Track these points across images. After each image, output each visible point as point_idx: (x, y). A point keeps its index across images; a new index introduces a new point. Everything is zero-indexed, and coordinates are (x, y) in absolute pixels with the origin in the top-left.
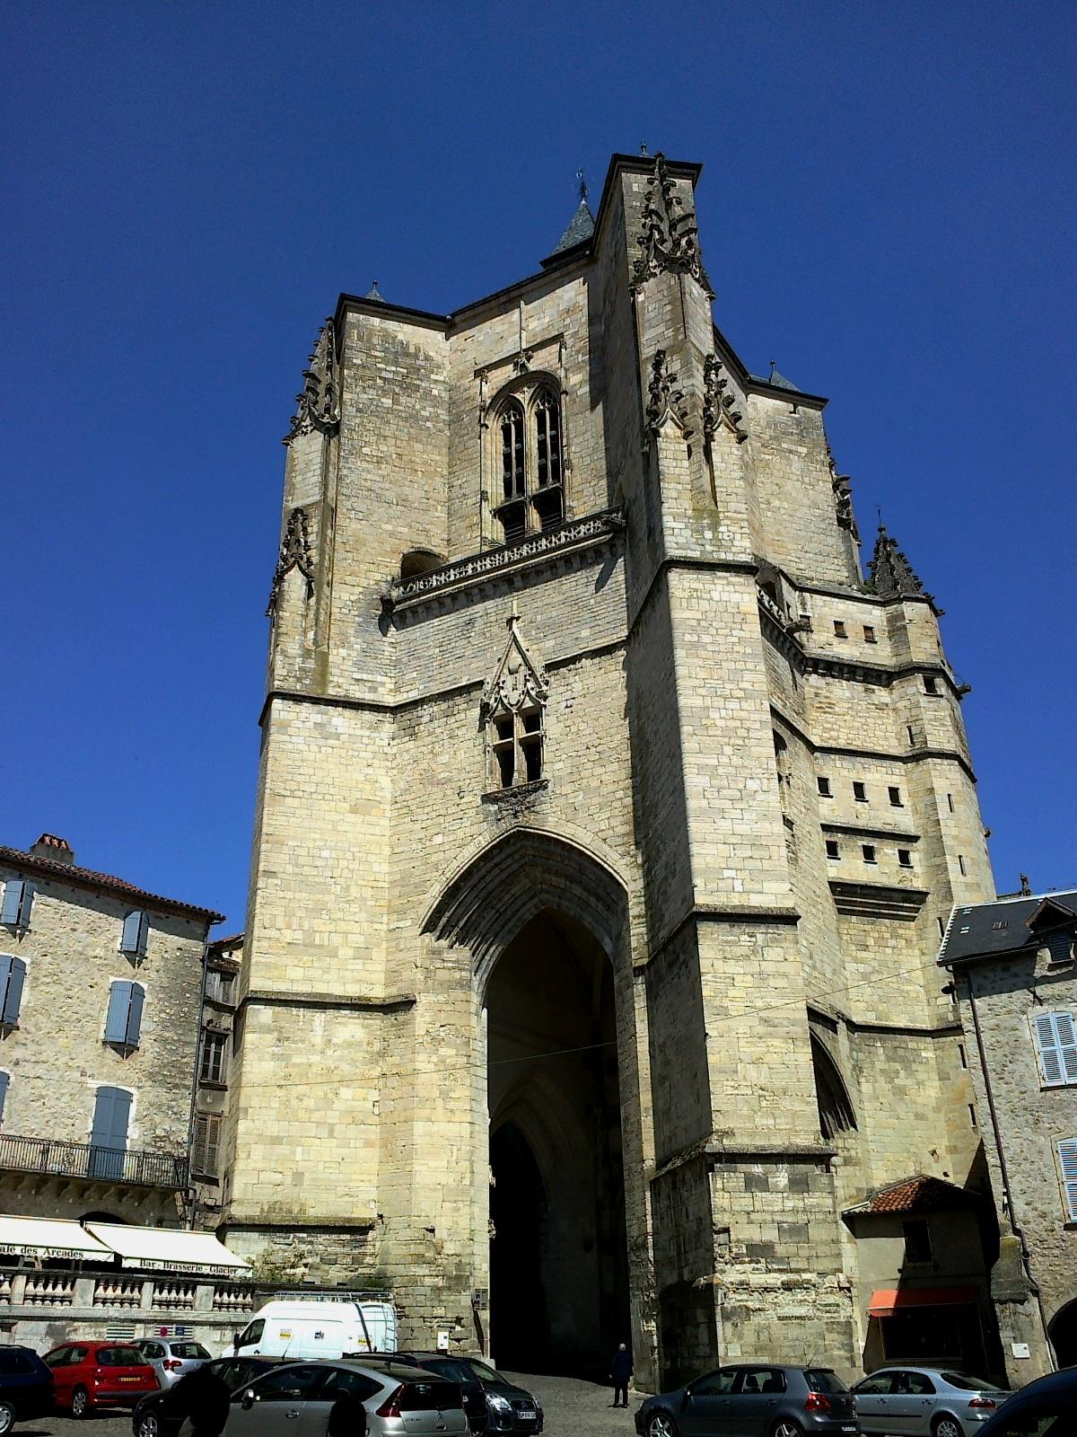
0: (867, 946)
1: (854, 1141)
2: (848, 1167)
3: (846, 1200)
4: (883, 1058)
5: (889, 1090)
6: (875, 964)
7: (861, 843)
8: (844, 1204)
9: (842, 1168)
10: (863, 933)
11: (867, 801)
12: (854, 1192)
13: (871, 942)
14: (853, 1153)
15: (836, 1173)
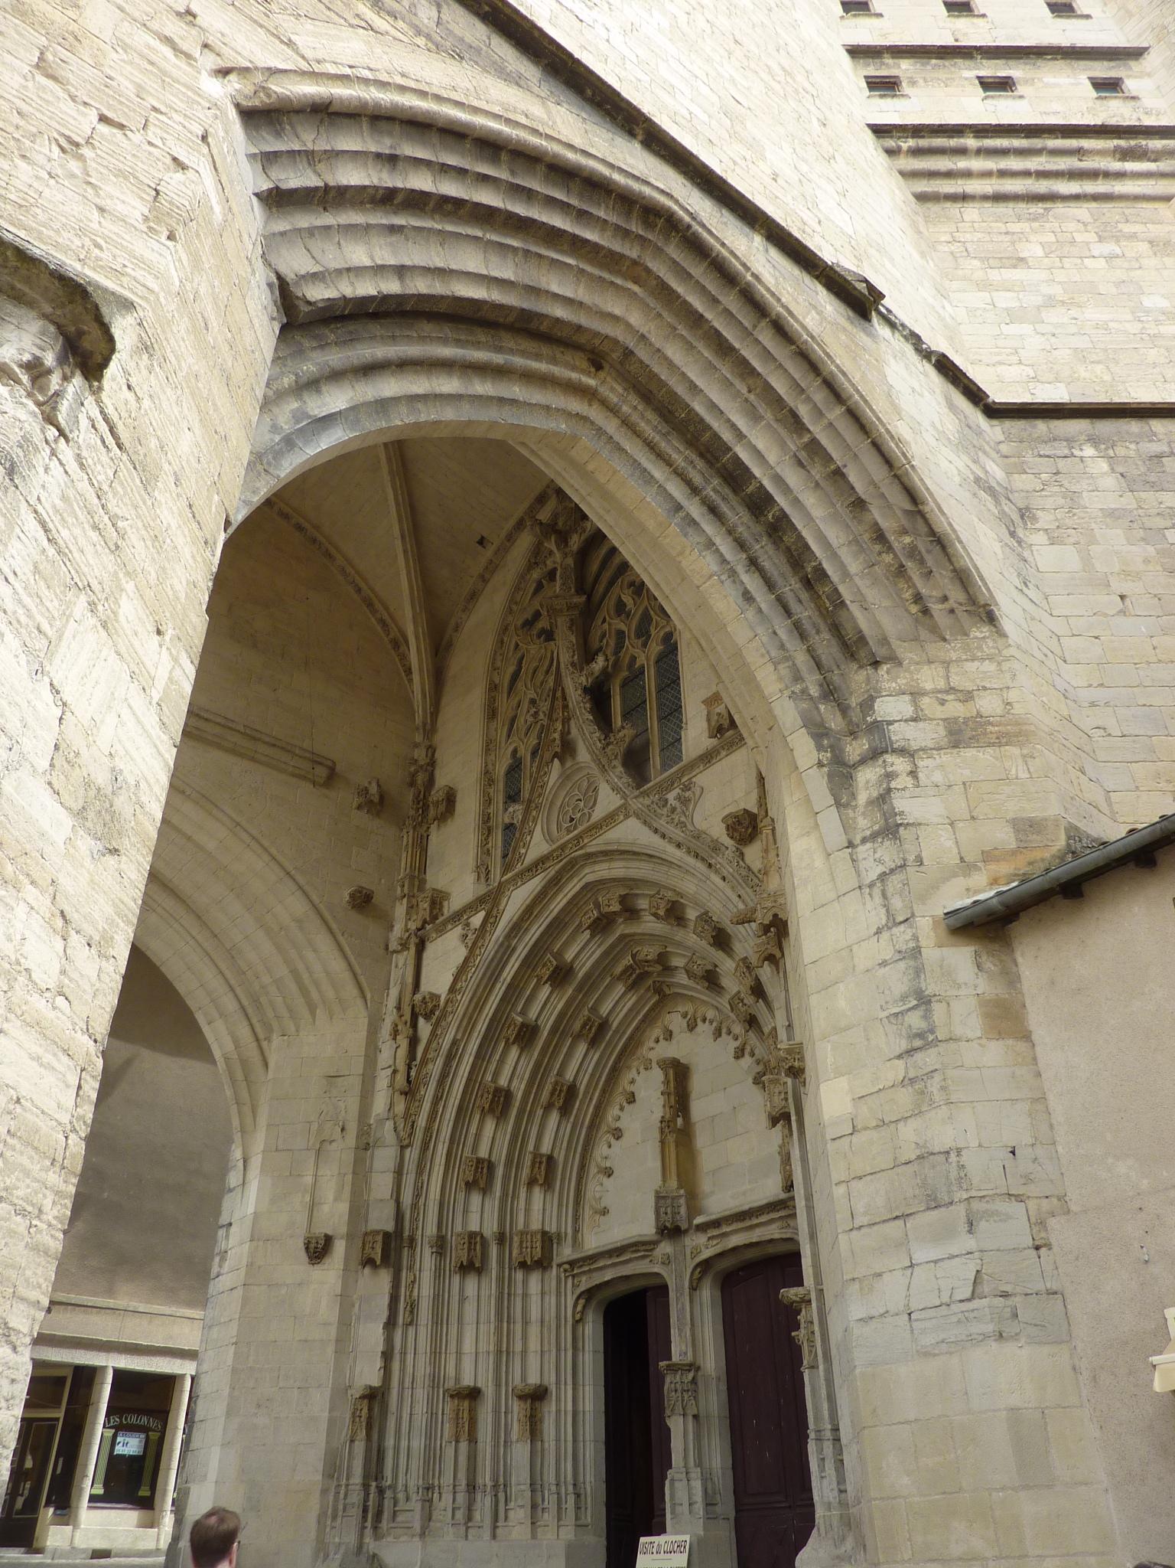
0: (1022, 259)
1: (989, 667)
2: (969, 753)
3: (966, 867)
4: (1110, 482)
5: (1147, 561)
6: (1057, 291)
7: (973, 73)
8: (960, 883)
9: (946, 758)
10: (1008, 238)
11: (984, 16)
12: (1004, 837)
13: (1032, 249)
14: (988, 705)
15: (913, 774)
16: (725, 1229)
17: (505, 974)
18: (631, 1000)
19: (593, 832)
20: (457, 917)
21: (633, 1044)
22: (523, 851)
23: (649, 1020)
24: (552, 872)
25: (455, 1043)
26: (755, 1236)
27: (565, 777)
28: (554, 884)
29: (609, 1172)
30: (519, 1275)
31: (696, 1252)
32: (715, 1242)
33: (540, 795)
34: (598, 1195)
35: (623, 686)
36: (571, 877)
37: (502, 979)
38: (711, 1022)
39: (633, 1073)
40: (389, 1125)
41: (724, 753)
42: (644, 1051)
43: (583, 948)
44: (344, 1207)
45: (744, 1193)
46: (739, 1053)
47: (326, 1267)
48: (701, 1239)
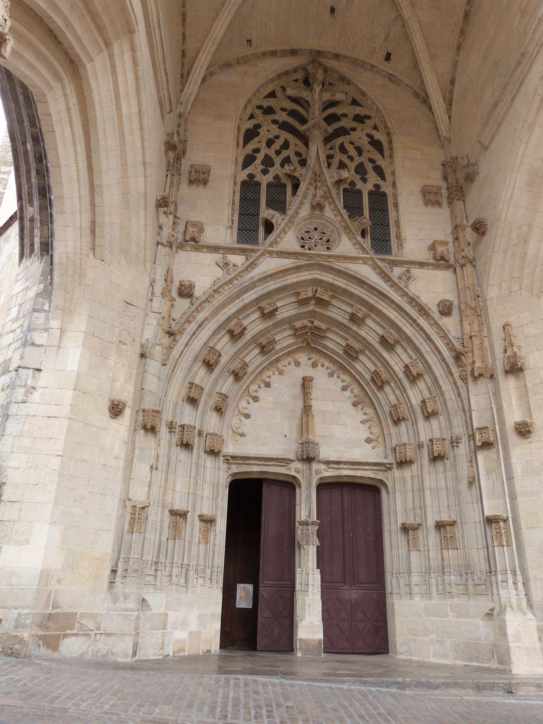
16: (342, 466)
17: (244, 297)
18: (291, 341)
19: (341, 259)
20: (215, 249)
21: (278, 360)
22: (279, 240)
23: (289, 354)
24: (302, 263)
25: (206, 319)
26: (359, 473)
27: (311, 217)
28: (297, 269)
29: (247, 416)
30: (203, 455)
31: (318, 472)
32: (332, 470)
33: (295, 217)
34: (237, 425)
35: (345, 190)
36: (306, 270)
37: (241, 298)
38: (327, 368)
39: (270, 373)
40: (158, 349)
41: (431, 267)
42: (279, 365)
43: (285, 305)
44: (130, 388)
45: (341, 451)
46: (344, 389)
47: (119, 422)
48: (323, 467)
